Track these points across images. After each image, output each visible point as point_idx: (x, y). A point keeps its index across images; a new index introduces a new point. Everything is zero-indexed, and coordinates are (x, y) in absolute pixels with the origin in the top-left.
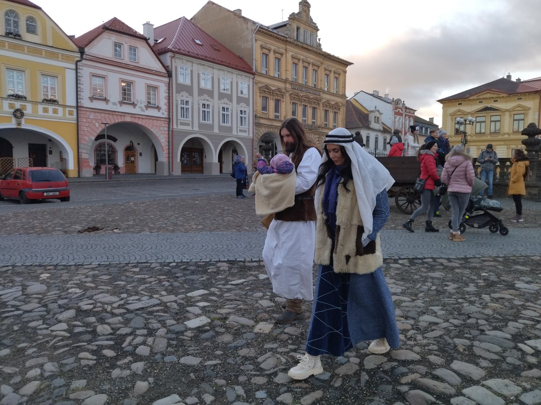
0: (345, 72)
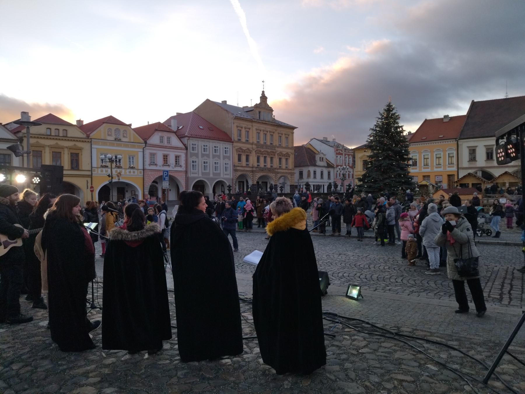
0: (293, 133)
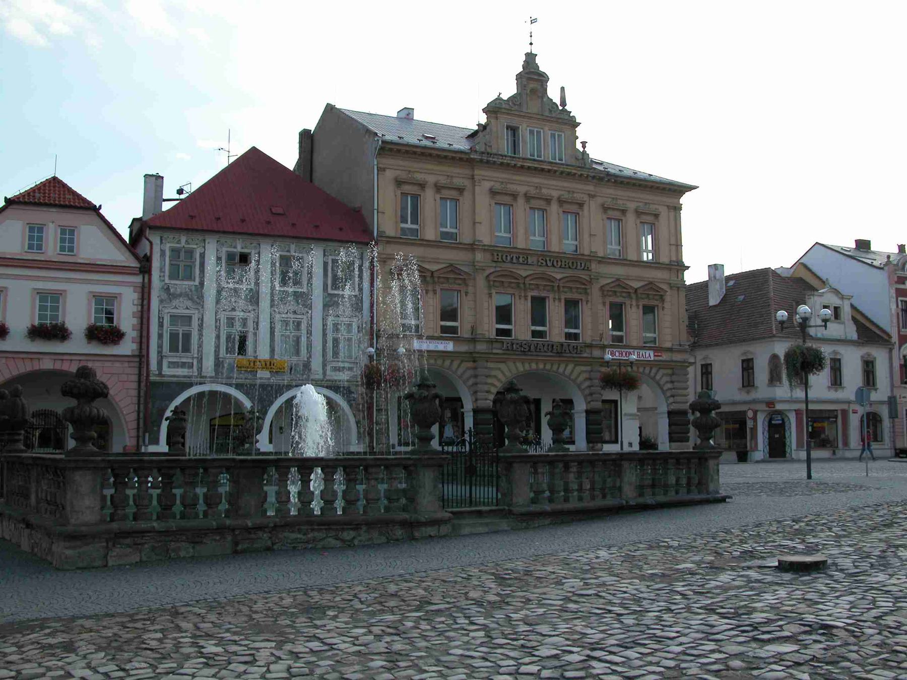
0: (678, 208)
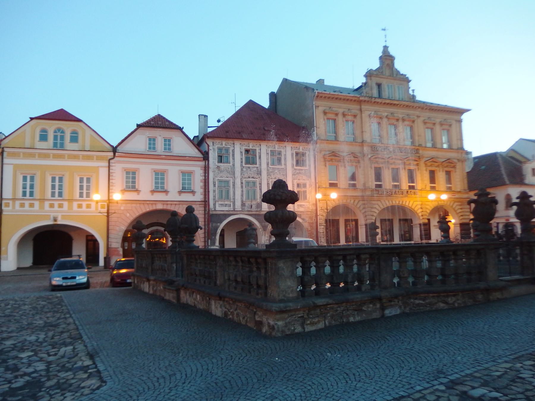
0: (460, 121)
